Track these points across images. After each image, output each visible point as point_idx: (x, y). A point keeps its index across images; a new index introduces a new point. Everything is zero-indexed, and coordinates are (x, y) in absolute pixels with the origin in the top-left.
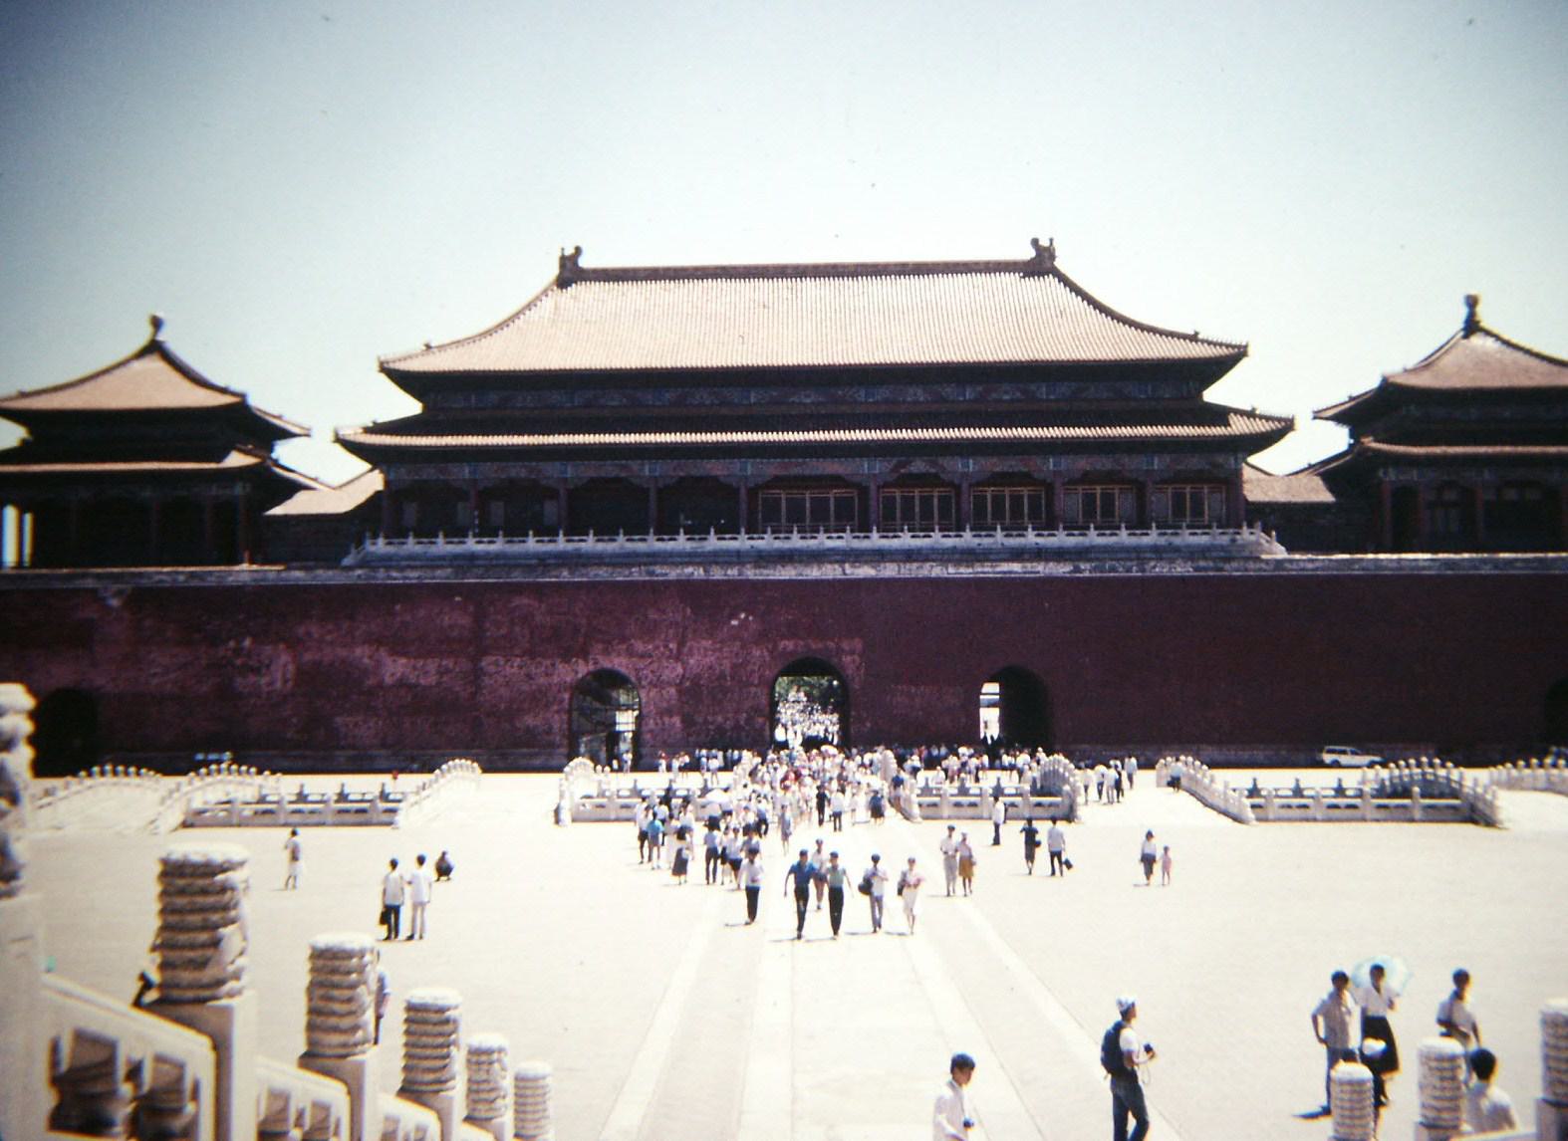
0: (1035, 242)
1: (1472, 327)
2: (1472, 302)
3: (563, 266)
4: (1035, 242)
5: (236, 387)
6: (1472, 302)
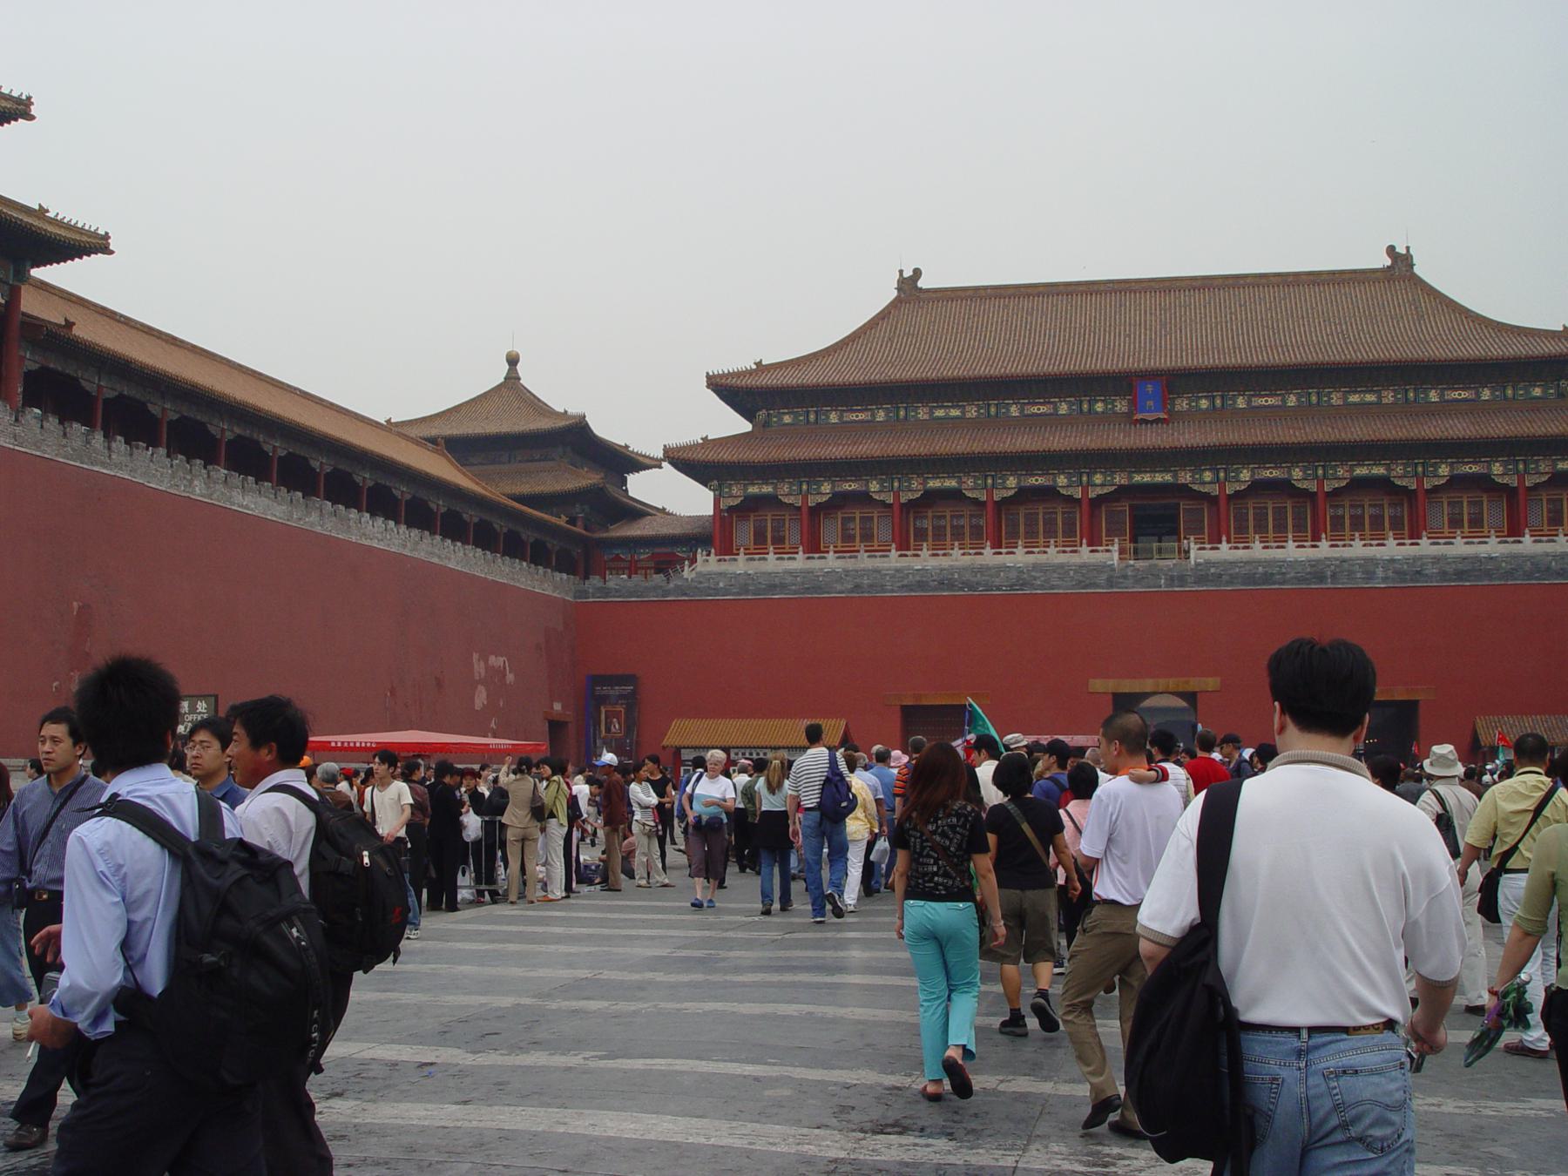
0: (1391, 250)
3: (899, 289)
4: (1391, 250)
5: (572, 410)
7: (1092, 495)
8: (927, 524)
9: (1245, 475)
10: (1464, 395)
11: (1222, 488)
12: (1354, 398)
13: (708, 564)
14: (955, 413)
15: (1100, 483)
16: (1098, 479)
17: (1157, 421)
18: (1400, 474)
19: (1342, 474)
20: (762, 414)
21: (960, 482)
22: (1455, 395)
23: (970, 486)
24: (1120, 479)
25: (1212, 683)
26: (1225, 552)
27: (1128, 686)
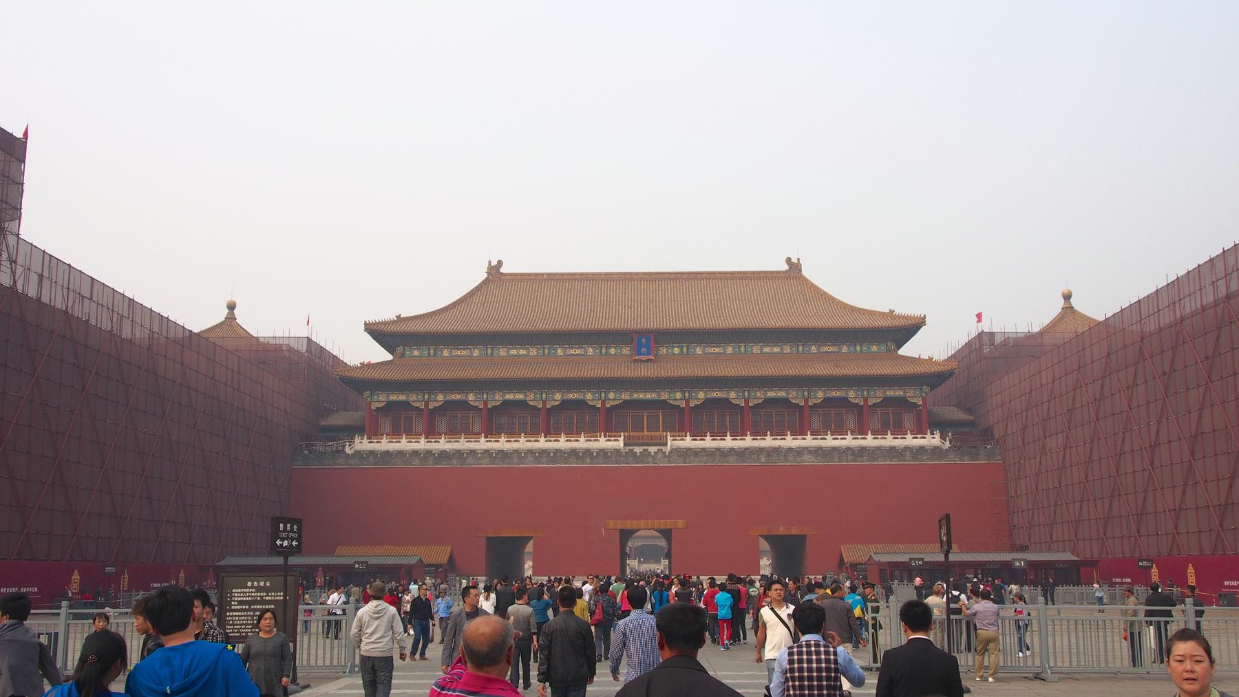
0: (789, 260)
1: (1068, 310)
2: (1067, 297)
4: (789, 260)
6: (1067, 297)
7: (607, 406)
8: (504, 420)
9: (701, 395)
10: (832, 349)
11: (687, 402)
12: (767, 350)
13: (362, 444)
14: (523, 352)
15: (613, 398)
16: (611, 395)
17: (648, 361)
18: (795, 396)
19: (758, 396)
20: (400, 349)
21: (526, 396)
22: (826, 349)
23: (532, 398)
24: (625, 396)
25: (680, 523)
26: (688, 442)
27: (628, 525)
